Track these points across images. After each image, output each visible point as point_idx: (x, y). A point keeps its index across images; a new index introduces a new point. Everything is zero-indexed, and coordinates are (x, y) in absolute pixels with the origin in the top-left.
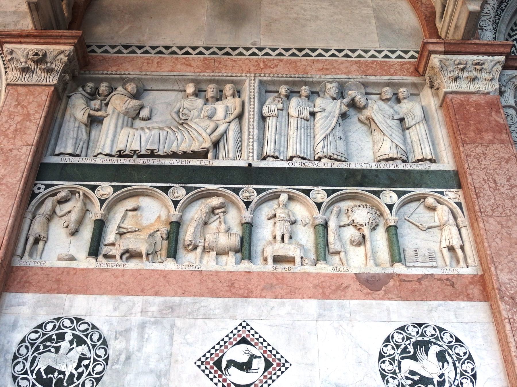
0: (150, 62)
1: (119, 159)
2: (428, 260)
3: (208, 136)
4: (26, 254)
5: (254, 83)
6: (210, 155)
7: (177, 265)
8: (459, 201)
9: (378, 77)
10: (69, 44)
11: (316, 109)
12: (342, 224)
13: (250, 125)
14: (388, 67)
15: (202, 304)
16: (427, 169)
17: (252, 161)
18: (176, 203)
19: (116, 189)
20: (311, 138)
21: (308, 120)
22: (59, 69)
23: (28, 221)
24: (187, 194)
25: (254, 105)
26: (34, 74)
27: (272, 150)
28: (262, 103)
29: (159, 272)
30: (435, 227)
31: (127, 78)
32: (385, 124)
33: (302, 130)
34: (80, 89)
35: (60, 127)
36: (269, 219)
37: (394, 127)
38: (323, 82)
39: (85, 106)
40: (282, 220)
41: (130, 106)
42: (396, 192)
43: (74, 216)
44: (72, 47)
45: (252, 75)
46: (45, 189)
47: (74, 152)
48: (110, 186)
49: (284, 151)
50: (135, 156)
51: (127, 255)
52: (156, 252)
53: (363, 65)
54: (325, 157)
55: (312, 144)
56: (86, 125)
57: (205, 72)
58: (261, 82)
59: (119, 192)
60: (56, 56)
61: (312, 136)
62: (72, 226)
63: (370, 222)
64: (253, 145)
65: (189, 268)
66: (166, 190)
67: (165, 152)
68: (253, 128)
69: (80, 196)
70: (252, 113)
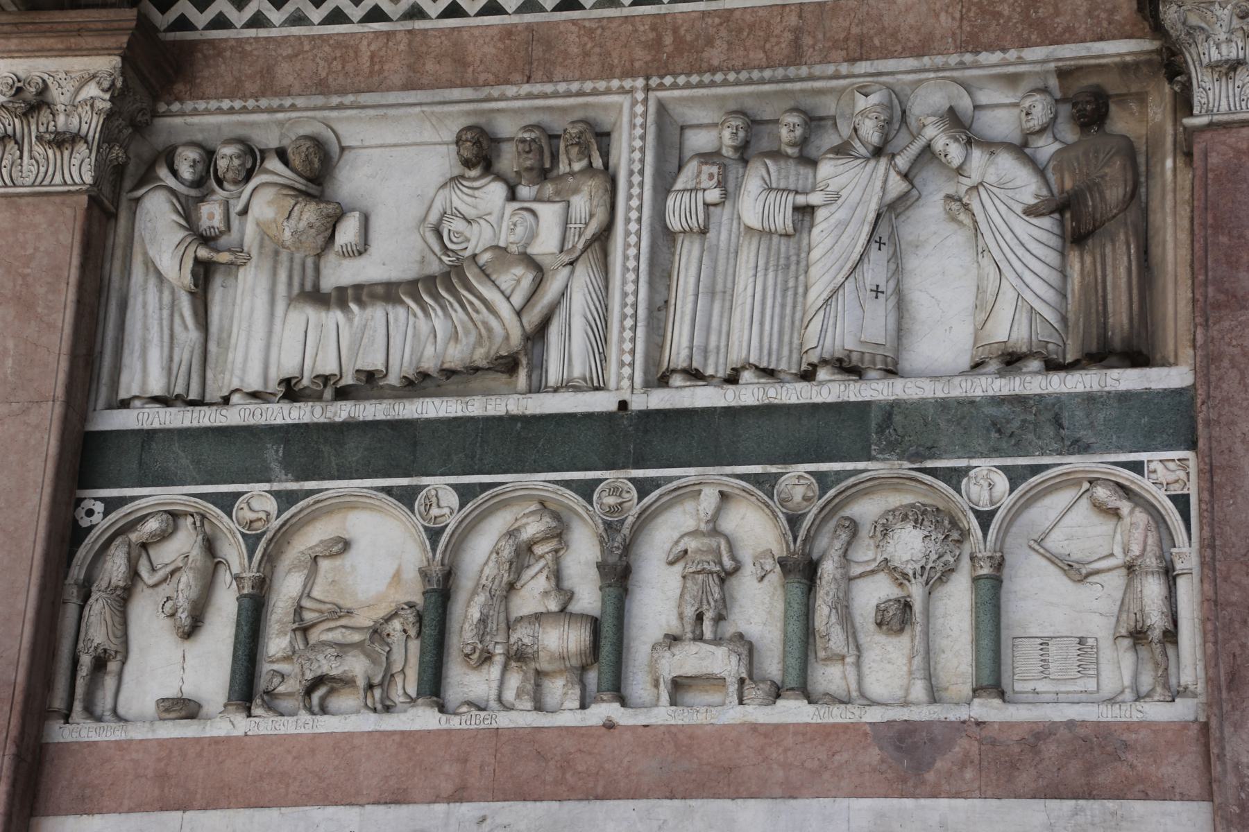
0: (352, 54)
2: (1073, 673)
3: (515, 318)
4: (78, 706)
5: (645, 114)
7: (440, 715)
8: (1185, 491)
9: (1012, 55)
10: (107, 51)
11: (815, 199)
12: (856, 570)
13: (628, 270)
14: (1051, 11)
15: (499, 820)
16: (1107, 389)
18: (434, 535)
19: (286, 499)
20: (796, 294)
21: (787, 235)
22: (91, 133)
23: (71, 610)
24: (462, 506)
26: (26, 154)
27: (684, 353)
28: (664, 187)
29: (397, 738)
30: (1109, 570)
31: (290, 119)
32: (1008, 236)
33: (771, 275)
34: (163, 172)
35: (123, 306)
36: (671, 563)
37: (1033, 246)
38: (842, 90)
40: (699, 572)
41: (303, 225)
42: (1004, 469)
43: (186, 585)
44: (116, 61)
45: (640, 82)
46: (106, 514)
47: (168, 391)
48: (269, 495)
49: (718, 348)
51: (322, 691)
52: (392, 676)
53: (973, 9)
54: (824, 362)
55: (798, 315)
56: (192, 293)
57: (507, 82)
58: (662, 108)
59: (294, 509)
60: (78, 91)
61: (801, 290)
62: (183, 616)
63: (928, 567)
64: (633, 340)
65: (468, 723)
66: (407, 497)
67: (404, 377)
68: (637, 281)
69: (194, 523)
70: (633, 227)
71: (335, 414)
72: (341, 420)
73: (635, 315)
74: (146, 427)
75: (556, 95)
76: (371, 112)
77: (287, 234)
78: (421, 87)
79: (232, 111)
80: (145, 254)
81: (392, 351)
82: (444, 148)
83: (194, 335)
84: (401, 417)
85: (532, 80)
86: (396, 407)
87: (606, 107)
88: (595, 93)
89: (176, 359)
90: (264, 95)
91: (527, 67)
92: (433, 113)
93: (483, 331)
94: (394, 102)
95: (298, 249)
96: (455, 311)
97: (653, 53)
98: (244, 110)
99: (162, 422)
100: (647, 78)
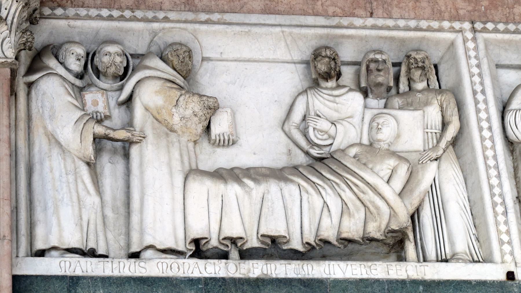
1: (194, 261)
3: (398, 200)
5: (476, 49)
6: (410, 249)
17: (513, 264)
25: (487, 110)
31: (163, 29)
34: (52, 63)
39: (79, 113)
45: (467, 25)
50: (234, 254)
57: (353, 15)
64: (506, 223)
67: (307, 243)
68: (499, 176)
70: (486, 134)
71: (249, 271)
72: (255, 276)
73: (504, 203)
74: (69, 273)
75: (397, 28)
76: (237, 28)
77: (176, 119)
78: (279, 13)
79: (110, 18)
80: (45, 128)
81: (290, 221)
82: (292, 66)
83: (97, 200)
84: (311, 276)
85: (374, 14)
86: (305, 267)
87: (438, 42)
88: (429, 29)
89: (85, 218)
90: (138, 8)
91: (368, 5)
92: (290, 34)
93: (372, 209)
94: (256, 22)
95: (183, 132)
96: (344, 191)
97: (473, 5)
98: (122, 18)
99: (85, 270)
100: (473, 23)
